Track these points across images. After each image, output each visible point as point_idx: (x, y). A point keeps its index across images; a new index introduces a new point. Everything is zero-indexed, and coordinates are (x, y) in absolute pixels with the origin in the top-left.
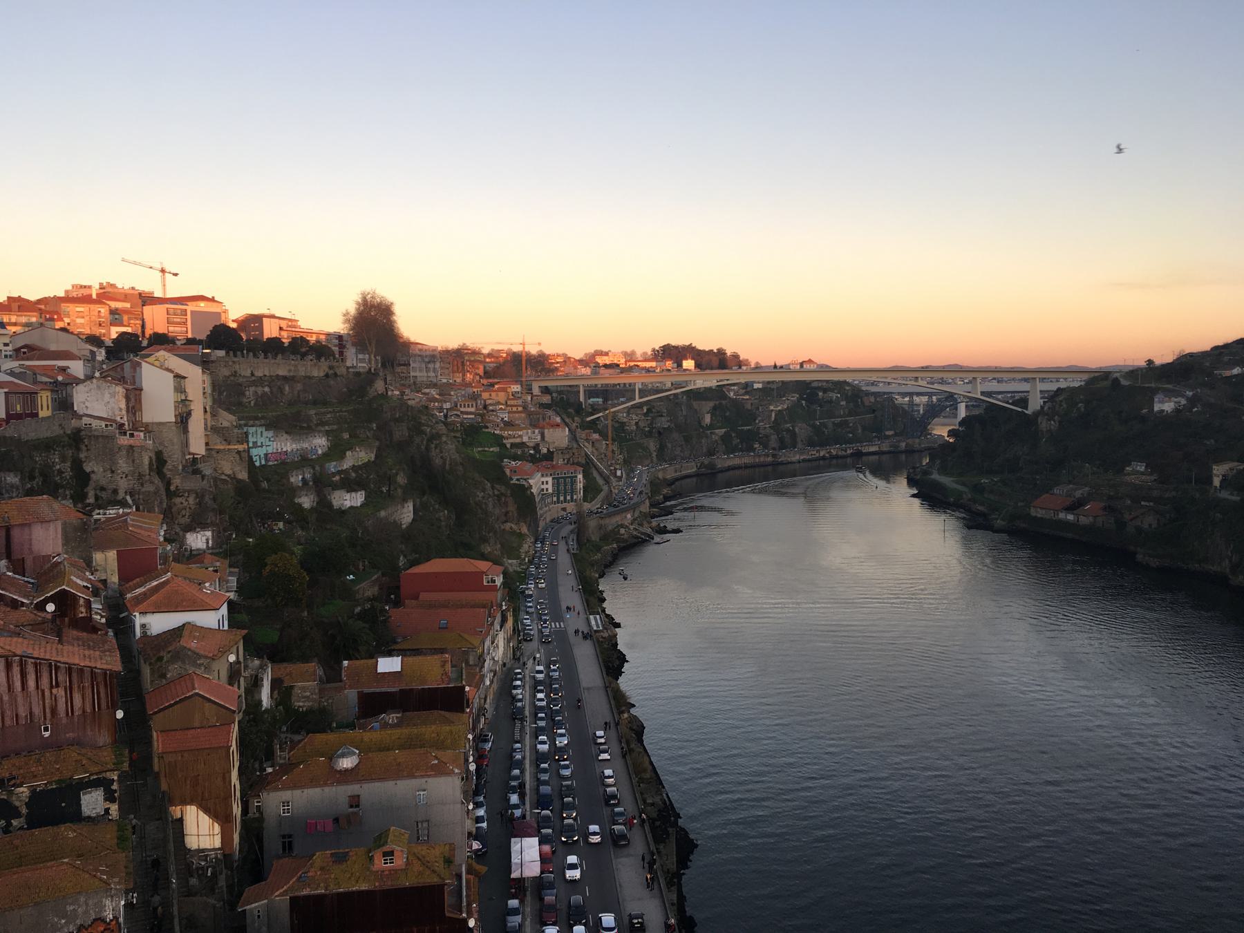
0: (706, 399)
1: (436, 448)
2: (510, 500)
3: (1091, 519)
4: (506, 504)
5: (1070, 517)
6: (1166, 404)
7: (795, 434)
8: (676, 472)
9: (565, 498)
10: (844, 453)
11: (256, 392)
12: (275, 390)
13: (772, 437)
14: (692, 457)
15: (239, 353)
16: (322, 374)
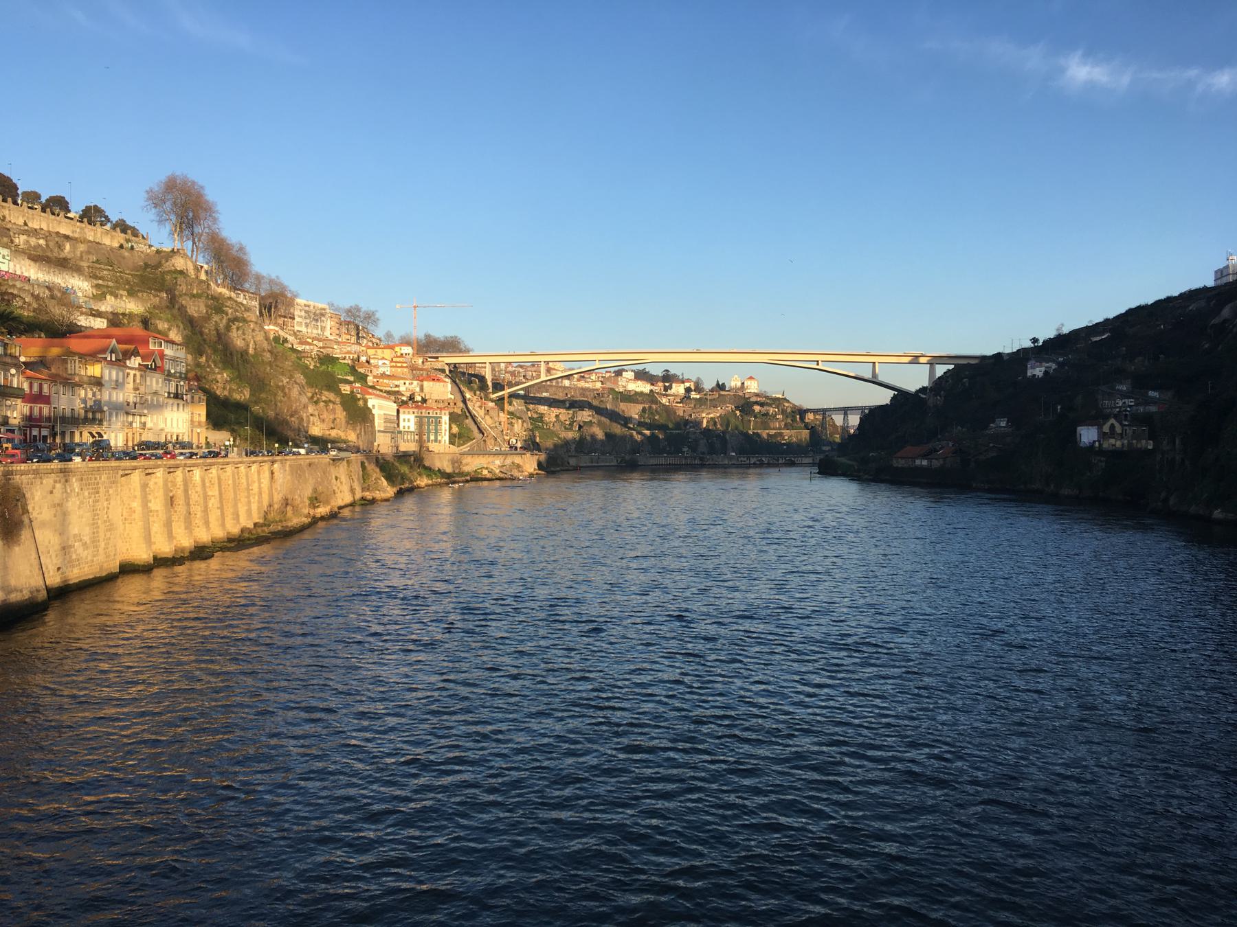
0: (636, 402)
1: (238, 329)
2: (339, 408)
3: (941, 461)
4: (334, 410)
5: (925, 463)
6: (1038, 369)
7: (726, 440)
8: (592, 462)
9: (429, 438)
10: (775, 462)
11: (28, 241)
12: (51, 244)
13: (701, 442)
14: (614, 452)
15: (9, 199)
16: (116, 245)
